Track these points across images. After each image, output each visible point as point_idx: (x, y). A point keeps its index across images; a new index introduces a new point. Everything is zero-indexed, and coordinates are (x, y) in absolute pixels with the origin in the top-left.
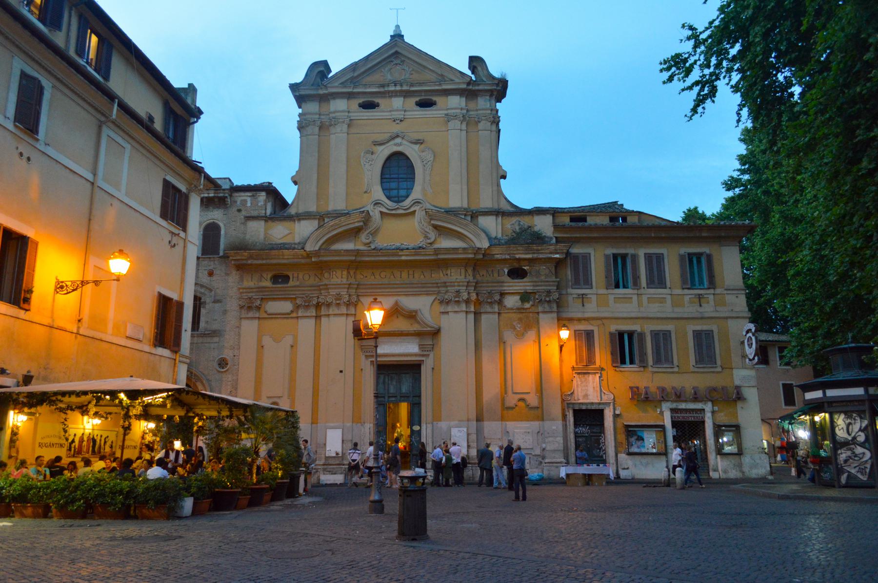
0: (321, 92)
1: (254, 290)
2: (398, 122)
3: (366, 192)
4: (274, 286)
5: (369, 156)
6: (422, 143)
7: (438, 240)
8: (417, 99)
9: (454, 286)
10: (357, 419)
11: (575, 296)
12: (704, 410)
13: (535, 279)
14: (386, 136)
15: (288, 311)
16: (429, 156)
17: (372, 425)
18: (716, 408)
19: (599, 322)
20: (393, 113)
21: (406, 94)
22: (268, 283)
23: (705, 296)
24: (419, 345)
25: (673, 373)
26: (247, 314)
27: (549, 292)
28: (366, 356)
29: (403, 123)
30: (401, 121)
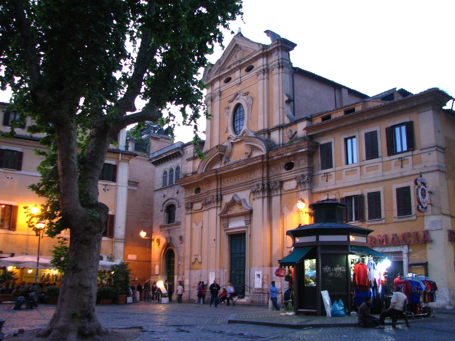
0: (209, 82)
1: (189, 198)
2: (239, 85)
3: (226, 132)
4: (196, 194)
5: (227, 110)
6: (248, 94)
7: (253, 153)
8: (245, 68)
9: (256, 182)
10: (221, 267)
11: (323, 175)
12: (402, 252)
13: (297, 168)
14: (233, 96)
15: (200, 208)
16: (250, 101)
17: (227, 270)
18: (411, 250)
19: (336, 192)
20: (236, 81)
21: (240, 67)
22: (193, 194)
23: (406, 158)
24: (245, 221)
25: (381, 224)
26: (187, 211)
27: (303, 176)
28: (225, 230)
29: (241, 85)
30: (240, 84)
